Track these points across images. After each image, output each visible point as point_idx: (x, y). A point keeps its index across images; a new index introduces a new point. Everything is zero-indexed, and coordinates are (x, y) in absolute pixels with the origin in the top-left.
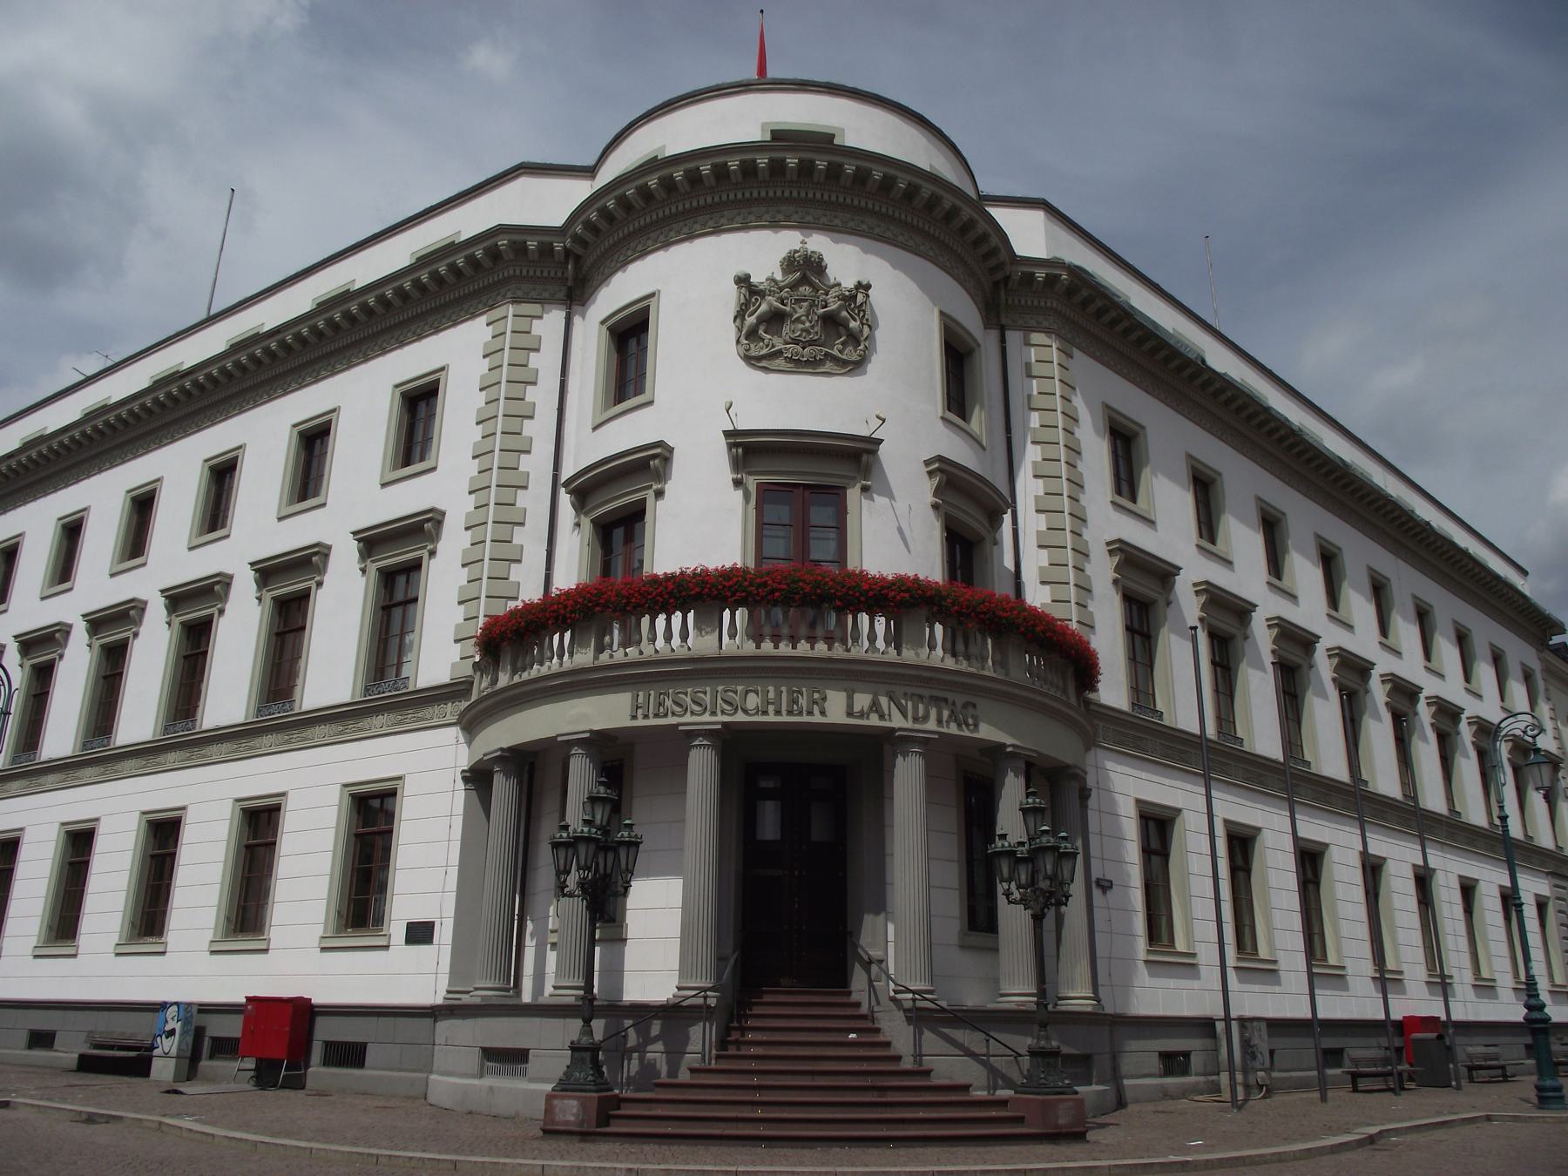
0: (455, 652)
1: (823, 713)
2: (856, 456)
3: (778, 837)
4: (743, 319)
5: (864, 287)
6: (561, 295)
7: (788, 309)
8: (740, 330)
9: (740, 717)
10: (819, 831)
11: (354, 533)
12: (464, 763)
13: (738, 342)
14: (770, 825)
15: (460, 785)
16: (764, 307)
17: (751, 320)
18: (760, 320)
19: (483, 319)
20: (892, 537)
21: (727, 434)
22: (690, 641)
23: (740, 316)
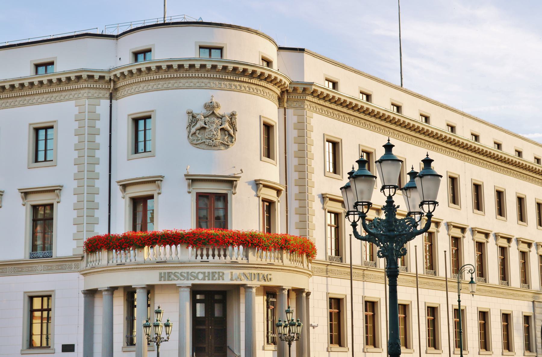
0: (74, 244)
1: (223, 279)
2: (231, 182)
3: (203, 315)
4: (190, 129)
5: (233, 115)
6: (108, 95)
7: (207, 126)
8: (189, 132)
9: (197, 282)
10: (217, 313)
11: (19, 190)
12: (83, 288)
13: (188, 137)
14: (200, 311)
15: (83, 295)
16: (198, 126)
17: (193, 130)
18: (197, 130)
19: (73, 103)
20: (245, 216)
21: (186, 175)
22: (179, 255)
23: (190, 126)
